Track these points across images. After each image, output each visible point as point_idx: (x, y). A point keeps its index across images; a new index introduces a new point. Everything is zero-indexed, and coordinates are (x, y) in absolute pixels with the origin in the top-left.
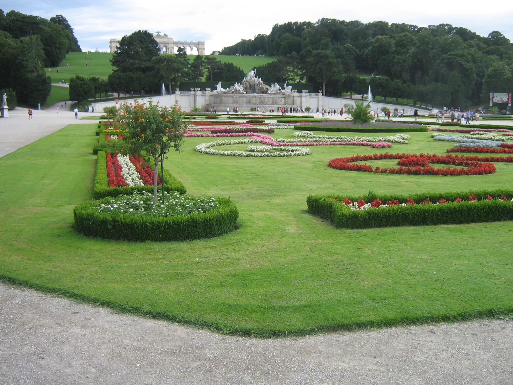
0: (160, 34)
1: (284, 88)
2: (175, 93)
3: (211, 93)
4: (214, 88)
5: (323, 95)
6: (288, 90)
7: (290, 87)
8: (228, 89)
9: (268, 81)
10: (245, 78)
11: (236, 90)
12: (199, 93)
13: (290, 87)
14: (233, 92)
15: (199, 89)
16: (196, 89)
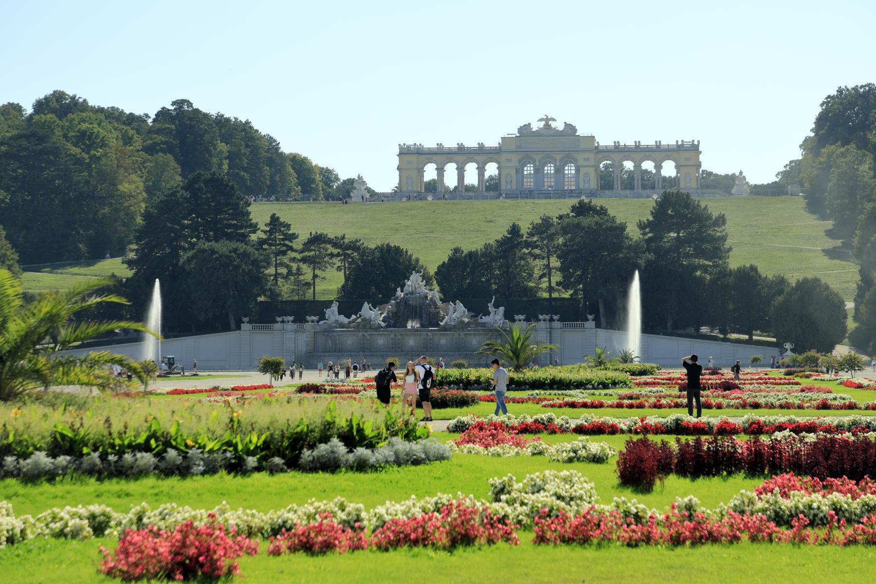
0: (553, 124)
1: (488, 313)
2: (239, 328)
3: (318, 329)
4: (322, 317)
5: (598, 326)
6: (496, 317)
7: (502, 309)
8: (354, 317)
9: (448, 296)
10: (399, 289)
11: (364, 320)
12: (291, 326)
13: (502, 309)
14: (358, 325)
15: (291, 318)
16: (286, 318)
